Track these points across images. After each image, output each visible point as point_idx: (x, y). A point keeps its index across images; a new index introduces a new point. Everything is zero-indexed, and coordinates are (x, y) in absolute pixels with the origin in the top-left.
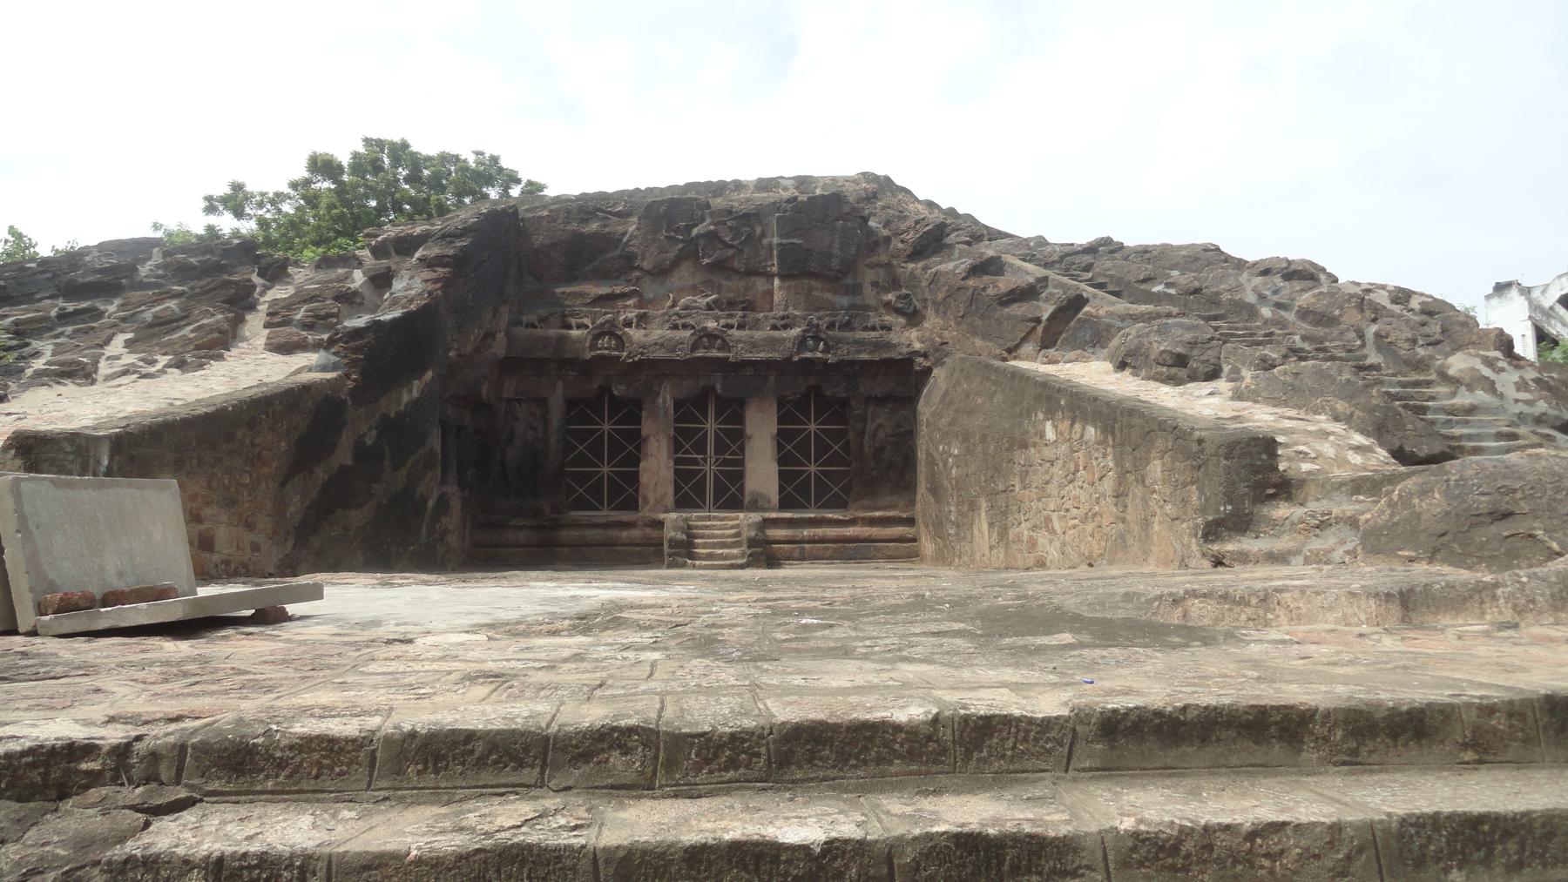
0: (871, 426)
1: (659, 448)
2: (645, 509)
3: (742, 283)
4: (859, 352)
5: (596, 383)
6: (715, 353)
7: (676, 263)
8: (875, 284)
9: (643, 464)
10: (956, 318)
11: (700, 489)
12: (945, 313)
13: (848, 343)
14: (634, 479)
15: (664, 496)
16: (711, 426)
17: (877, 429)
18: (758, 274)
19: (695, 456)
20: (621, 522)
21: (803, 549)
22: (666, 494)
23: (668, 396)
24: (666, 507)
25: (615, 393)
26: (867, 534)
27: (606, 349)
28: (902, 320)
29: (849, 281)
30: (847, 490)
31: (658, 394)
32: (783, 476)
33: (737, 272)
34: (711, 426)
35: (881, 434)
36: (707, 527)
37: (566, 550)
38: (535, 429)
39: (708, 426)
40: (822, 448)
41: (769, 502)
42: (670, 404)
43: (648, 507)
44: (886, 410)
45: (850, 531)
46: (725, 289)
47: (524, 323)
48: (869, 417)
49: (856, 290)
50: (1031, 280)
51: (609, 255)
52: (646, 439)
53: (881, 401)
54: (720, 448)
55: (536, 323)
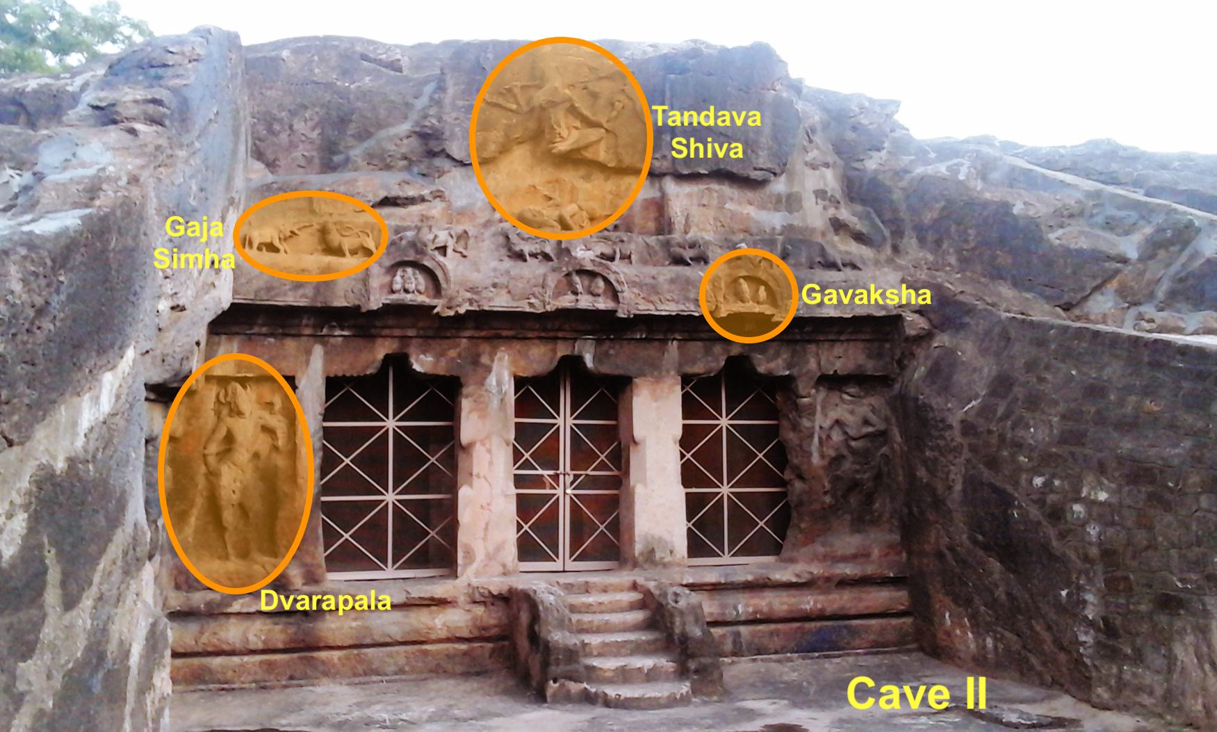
0: (821, 421)
1: (491, 463)
5: (382, 349)
6: (585, 302)
7: (504, 149)
8: (820, 194)
9: (464, 492)
11: (548, 527)
12: (938, 243)
14: (447, 514)
15: (499, 548)
16: (565, 421)
19: (540, 472)
20: (432, 599)
21: (738, 634)
22: (504, 543)
24: (504, 566)
25: (417, 367)
26: (836, 606)
27: (406, 291)
29: (779, 186)
30: (782, 524)
31: (488, 370)
32: (693, 504)
33: (602, 167)
34: (565, 421)
36: (588, 609)
37: (336, 654)
38: (268, 430)
39: (560, 421)
40: (739, 456)
41: (671, 552)
42: (509, 387)
43: (474, 566)
44: (846, 397)
45: (809, 602)
47: (255, 245)
48: (819, 408)
50: (1079, 195)
51: (393, 131)
52: (471, 445)
54: (581, 457)
55: (277, 243)
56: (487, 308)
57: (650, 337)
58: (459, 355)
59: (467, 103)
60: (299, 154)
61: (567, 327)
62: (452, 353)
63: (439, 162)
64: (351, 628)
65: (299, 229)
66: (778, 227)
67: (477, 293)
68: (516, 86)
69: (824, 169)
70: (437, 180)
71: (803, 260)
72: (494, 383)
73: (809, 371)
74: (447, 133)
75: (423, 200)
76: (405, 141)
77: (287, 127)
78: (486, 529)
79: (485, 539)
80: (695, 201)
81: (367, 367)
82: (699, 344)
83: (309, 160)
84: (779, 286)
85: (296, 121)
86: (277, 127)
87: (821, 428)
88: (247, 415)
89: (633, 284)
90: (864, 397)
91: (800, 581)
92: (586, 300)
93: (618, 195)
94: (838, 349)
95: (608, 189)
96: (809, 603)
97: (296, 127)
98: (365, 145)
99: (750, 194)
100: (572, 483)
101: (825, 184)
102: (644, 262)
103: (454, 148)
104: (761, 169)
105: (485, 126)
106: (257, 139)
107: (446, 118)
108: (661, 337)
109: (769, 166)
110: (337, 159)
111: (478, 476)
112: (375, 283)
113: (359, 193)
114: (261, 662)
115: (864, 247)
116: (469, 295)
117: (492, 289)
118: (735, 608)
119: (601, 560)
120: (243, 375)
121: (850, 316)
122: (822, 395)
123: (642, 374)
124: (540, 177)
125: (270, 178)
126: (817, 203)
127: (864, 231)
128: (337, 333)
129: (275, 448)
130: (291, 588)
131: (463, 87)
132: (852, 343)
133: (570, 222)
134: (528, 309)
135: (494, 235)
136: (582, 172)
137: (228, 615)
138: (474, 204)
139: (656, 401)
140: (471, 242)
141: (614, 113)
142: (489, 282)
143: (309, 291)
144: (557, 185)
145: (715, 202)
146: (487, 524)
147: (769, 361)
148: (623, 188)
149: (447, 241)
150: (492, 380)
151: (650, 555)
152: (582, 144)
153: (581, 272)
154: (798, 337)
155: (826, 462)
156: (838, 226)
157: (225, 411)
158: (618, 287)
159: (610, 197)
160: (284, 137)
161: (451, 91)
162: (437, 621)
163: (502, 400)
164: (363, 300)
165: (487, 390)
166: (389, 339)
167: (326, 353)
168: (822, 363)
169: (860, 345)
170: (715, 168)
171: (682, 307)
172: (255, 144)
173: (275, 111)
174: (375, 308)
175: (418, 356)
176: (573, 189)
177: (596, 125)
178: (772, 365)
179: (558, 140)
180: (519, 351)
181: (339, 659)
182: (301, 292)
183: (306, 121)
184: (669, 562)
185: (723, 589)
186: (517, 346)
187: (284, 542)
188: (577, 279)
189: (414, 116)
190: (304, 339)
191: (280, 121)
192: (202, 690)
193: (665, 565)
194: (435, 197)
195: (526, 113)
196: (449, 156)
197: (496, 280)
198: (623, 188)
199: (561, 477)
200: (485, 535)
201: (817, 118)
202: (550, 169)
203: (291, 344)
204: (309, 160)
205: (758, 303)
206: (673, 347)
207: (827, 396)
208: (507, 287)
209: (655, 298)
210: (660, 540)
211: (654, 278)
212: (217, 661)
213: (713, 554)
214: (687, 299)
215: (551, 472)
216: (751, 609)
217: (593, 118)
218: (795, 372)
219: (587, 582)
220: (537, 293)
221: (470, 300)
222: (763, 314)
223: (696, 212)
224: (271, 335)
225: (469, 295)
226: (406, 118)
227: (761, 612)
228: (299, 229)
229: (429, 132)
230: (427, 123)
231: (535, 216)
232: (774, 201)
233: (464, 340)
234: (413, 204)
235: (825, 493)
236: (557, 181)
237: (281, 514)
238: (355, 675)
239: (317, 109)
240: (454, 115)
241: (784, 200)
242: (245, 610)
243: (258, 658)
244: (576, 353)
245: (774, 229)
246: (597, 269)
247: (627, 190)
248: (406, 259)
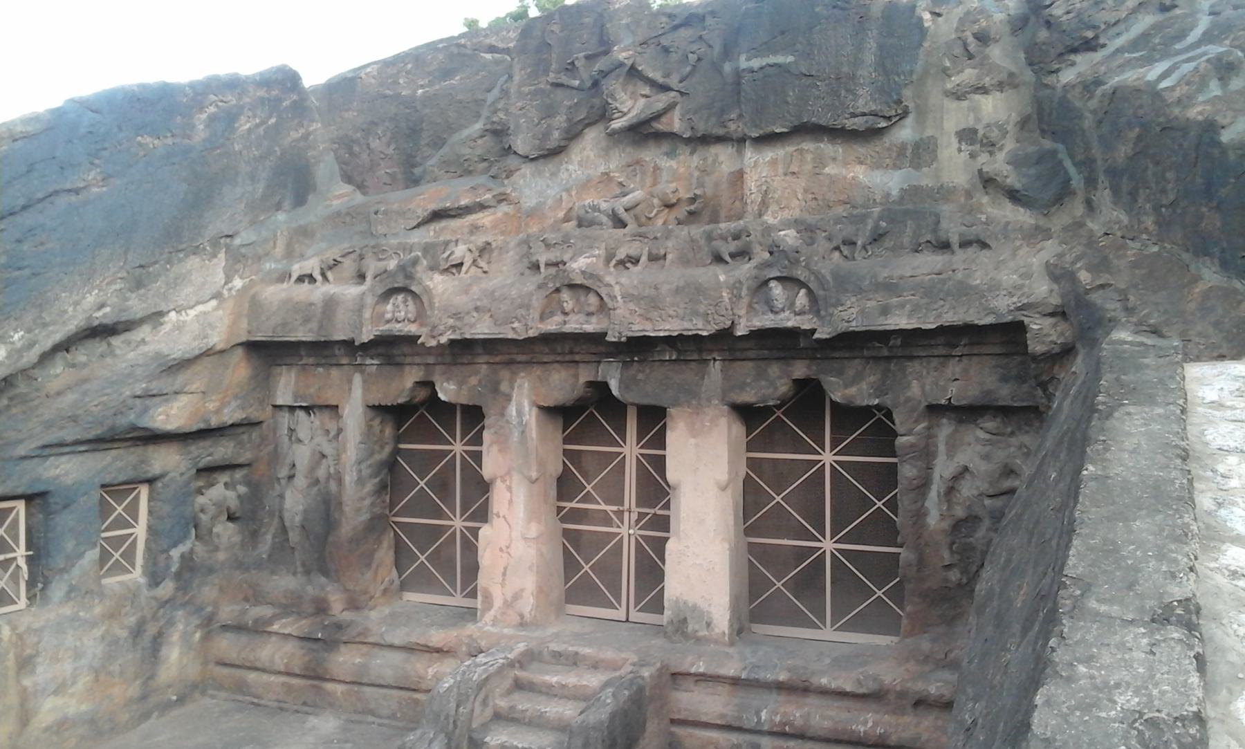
0: (943, 469)
1: (511, 502)
2: (489, 617)
3: (695, 160)
4: (885, 311)
5: (411, 377)
7: (573, 134)
8: (967, 135)
10: (1157, 209)
11: (611, 571)
12: (1133, 195)
13: (859, 291)
15: (517, 596)
17: (957, 477)
18: (720, 140)
19: (603, 507)
22: (522, 590)
23: (526, 404)
24: (522, 616)
25: (442, 396)
28: (1022, 217)
29: (905, 133)
31: (508, 398)
35: (967, 489)
37: (339, 688)
41: (709, 625)
42: (531, 416)
43: (492, 612)
46: (665, 176)
47: (295, 276)
48: (942, 448)
49: (922, 153)
51: (465, 133)
53: (968, 413)
56: (468, 336)
57: (682, 358)
58: (480, 381)
59: (533, 88)
60: (383, 172)
61: (577, 349)
62: (473, 381)
63: (512, 161)
64: (354, 664)
65: (343, 256)
66: (895, 192)
67: (459, 319)
68: (577, 58)
69: (977, 97)
70: (506, 182)
71: (906, 240)
72: (514, 413)
73: (908, 400)
74: (512, 127)
75: (482, 207)
76: (480, 142)
77: (364, 147)
78: (504, 574)
79: (503, 585)
80: (781, 171)
81: (399, 396)
82: (750, 364)
83: (393, 176)
84: (824, 289)
85: (371, 139)
86: (356, 149)
87: (941, 477)
88: (306, 442)
89: (628, 297)
90: (1012, 433)
91: (862, 691)
92: (577, 322)
93: (704, 171)
94: (954, 368)
95: (693, 165)
96: (865, 723)
97: (373, 146)
98: (442, 152)
99: (861, 150)
100: (638, 521)
101: (978, 120)
102: (684, 261)
103: (519, 142)
104: (864, 114)
105: (549, 112)
106: (342, 162)
107: (513, 110)
108: (695, 357)
109: (874, 108)
110: (417, 171)
111: (498, 516)
112: (367, 314)
113: (409, 209)
114: (283, 684)
115: (1022, 210)
116: (451, 322)
117: (475, 314)
118: (758, 713)
119: (654, 613)
121: (934, 326)
122: (945, 429)
123: (676, 404)
124: (615, 162)
125: (359, 198)
126: (960, 150)
127: (1018, 186)
128: (368, 361)
130: (330, 613)
131: (529, 70)
132: (975, 359)
133: (624, 216)
134: (511, 335)
135: (519, 245)
136: (665, 147)
137: (270, 633)
138: (544, 203)
139: (694, 437)
140: (495, 254)
141: (688, 69)
142: (471, 306)
143: (314, 325)
144: (638, 167)
145: (808, 167)
146: (505, 569)
147: (846, 386)
148: (710, 160)
149: (464, 257)
150: (512, 410)
151: (681, 624)
152: (648, 113)
153: (572, 287)
154: (885, 353)
155: (946, 525)
156: (988, 182)
158: (610, 304)
159: (696, 174)
160: (365, 156)
161: (517, 78)
162: (430, 670)
163: (523, 432)
164: (356, 332)
165: (508, 422)
166: (415, 366)
167: (365, 382)
168: (928, 387)
169: (991, 362)
170: (796, 123)
171: (687, 325)
172: (341, 169)
173: (350, 133)
174: (366, 341)
175: (442, 384)
176: (657, 169)
177: (665, 88)
178: (852, 391)
179: (616, 116)
180: (539, 378)
181: (342, 693)
182: (309, 326)
183: (379, 138)
184: (704, 637)
185: (753, 686)
186: (538, 371)
188: (566, 295)
189: (485, 113)
190: (346, 368)
191: (356, 142)
192: (239, 701)
193: (698, 640)
194: (500, 201)
195: (590, 89)
196: (515, 153)
197: (479, 304)
198: (710, 160)
199: (626, 515)
200: (503, 580)
201: (999, 16)
202: (629, 149)
203: (335, 372)
204: (393, 176)
205: (797, 314)
206: (715, 369)
207: (956, 431)
208: (490, 310)
209: (654, 314)
210: (695, 607)
211: (656, 288)
212: (252, 676)
213: (813, 626)
214: (696, 313)
215: (615, 508)
216: (778, 719)
217: (661, 80)
218: (888, 401)
219: (577, 653)
220: (519, 317)
221: (451, 327)
222: (799, 328)
223: (778, 183)
224: (318, 365)
225: (451, 322)
226: (478, 116)
227: (791, 725)
228: (343, 256)
229: (499, 128)
230: (495, 119)
231: (587, 212)
232: (894, 155)
233: (484, 366)
234: (471, 213)
235: (948, 567)
236: (638, 162)
237: (331, 539)
238: (355, 712)
239: (387, 124)
240: (519, 104)
241: (909, 152)
242: (281, 631)
243: (283, 679)
244: (599, 379)
245: (888, 195)
246: (586, 282)
247: (714, 161)
248: (396, 285)
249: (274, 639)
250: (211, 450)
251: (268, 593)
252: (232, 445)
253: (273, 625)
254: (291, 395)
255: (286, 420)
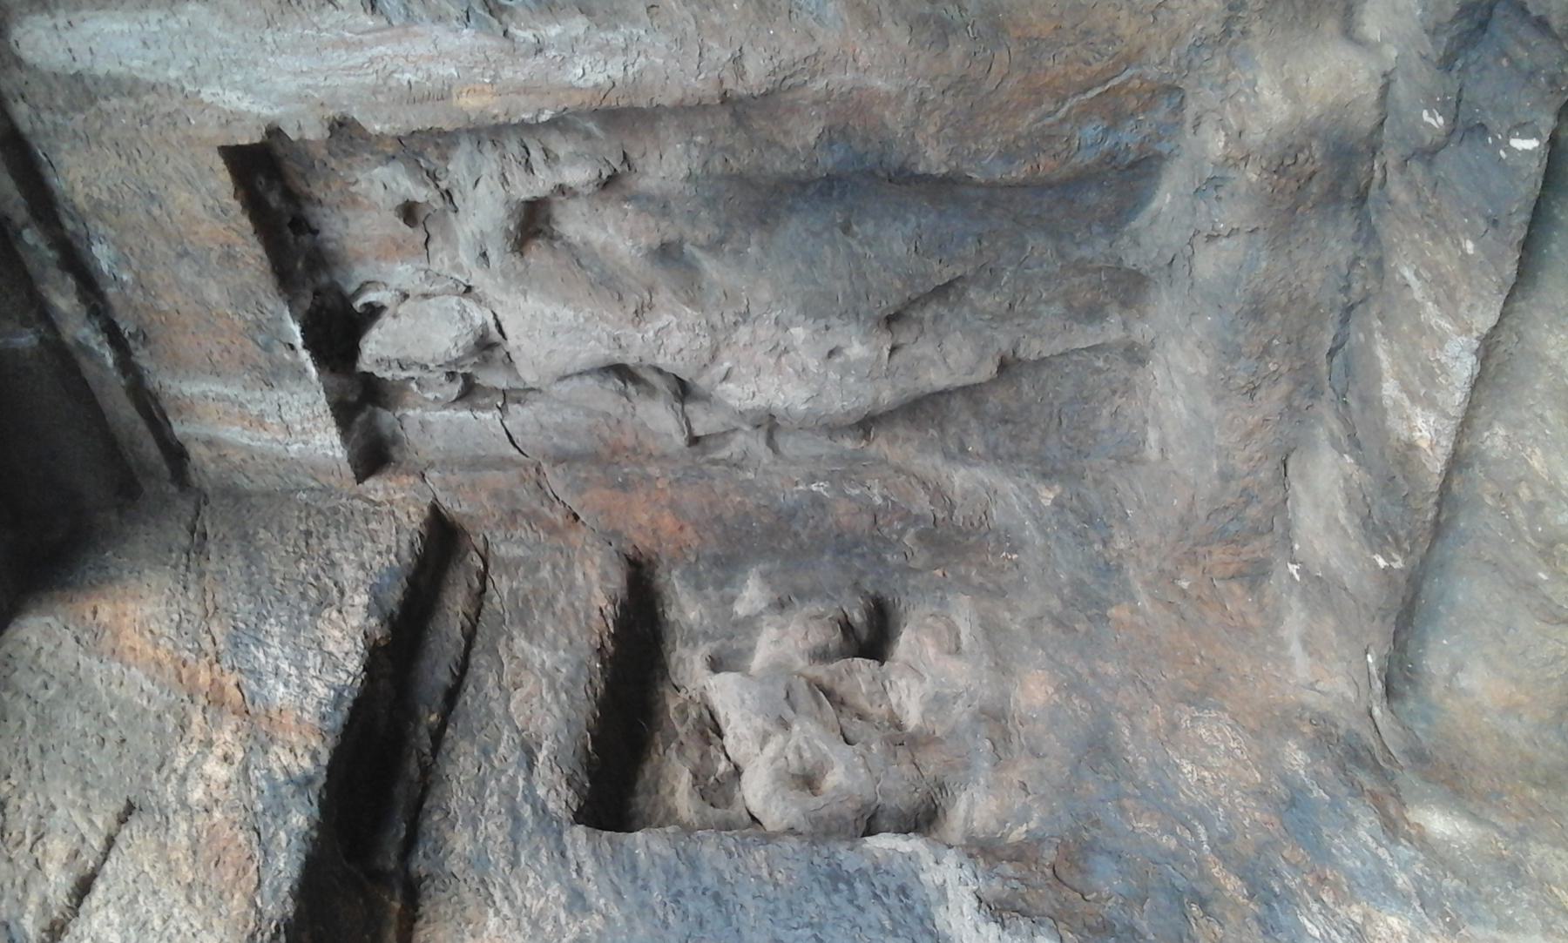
88: (480, 316)
120: (305, 355)
129: (609, 184)
130: (1365, 119)
137: (1457, 462)
157: (492, 378)
187: (1090, 131)
237: (933, 158)
242: (1457, 398)
249: (1495, 439)
250: (506, 747)
251: (1225, 477)
252: (521, 643)
253: (1412, 446)
254: (279, 394)
255: (437, 416)
